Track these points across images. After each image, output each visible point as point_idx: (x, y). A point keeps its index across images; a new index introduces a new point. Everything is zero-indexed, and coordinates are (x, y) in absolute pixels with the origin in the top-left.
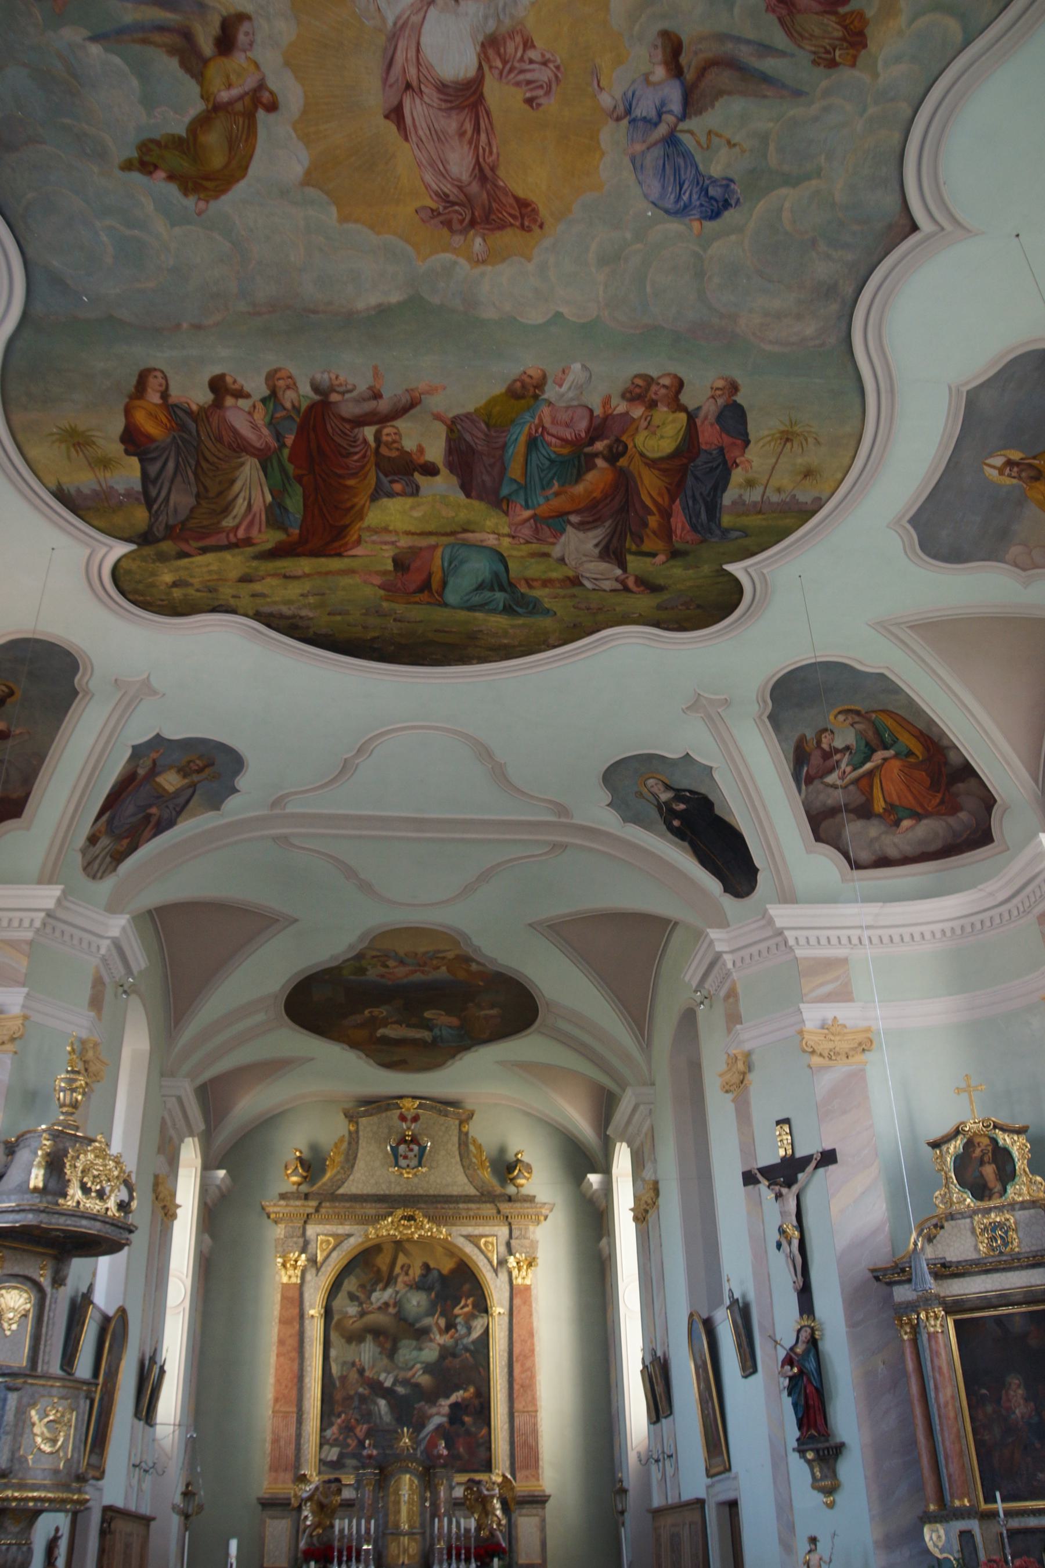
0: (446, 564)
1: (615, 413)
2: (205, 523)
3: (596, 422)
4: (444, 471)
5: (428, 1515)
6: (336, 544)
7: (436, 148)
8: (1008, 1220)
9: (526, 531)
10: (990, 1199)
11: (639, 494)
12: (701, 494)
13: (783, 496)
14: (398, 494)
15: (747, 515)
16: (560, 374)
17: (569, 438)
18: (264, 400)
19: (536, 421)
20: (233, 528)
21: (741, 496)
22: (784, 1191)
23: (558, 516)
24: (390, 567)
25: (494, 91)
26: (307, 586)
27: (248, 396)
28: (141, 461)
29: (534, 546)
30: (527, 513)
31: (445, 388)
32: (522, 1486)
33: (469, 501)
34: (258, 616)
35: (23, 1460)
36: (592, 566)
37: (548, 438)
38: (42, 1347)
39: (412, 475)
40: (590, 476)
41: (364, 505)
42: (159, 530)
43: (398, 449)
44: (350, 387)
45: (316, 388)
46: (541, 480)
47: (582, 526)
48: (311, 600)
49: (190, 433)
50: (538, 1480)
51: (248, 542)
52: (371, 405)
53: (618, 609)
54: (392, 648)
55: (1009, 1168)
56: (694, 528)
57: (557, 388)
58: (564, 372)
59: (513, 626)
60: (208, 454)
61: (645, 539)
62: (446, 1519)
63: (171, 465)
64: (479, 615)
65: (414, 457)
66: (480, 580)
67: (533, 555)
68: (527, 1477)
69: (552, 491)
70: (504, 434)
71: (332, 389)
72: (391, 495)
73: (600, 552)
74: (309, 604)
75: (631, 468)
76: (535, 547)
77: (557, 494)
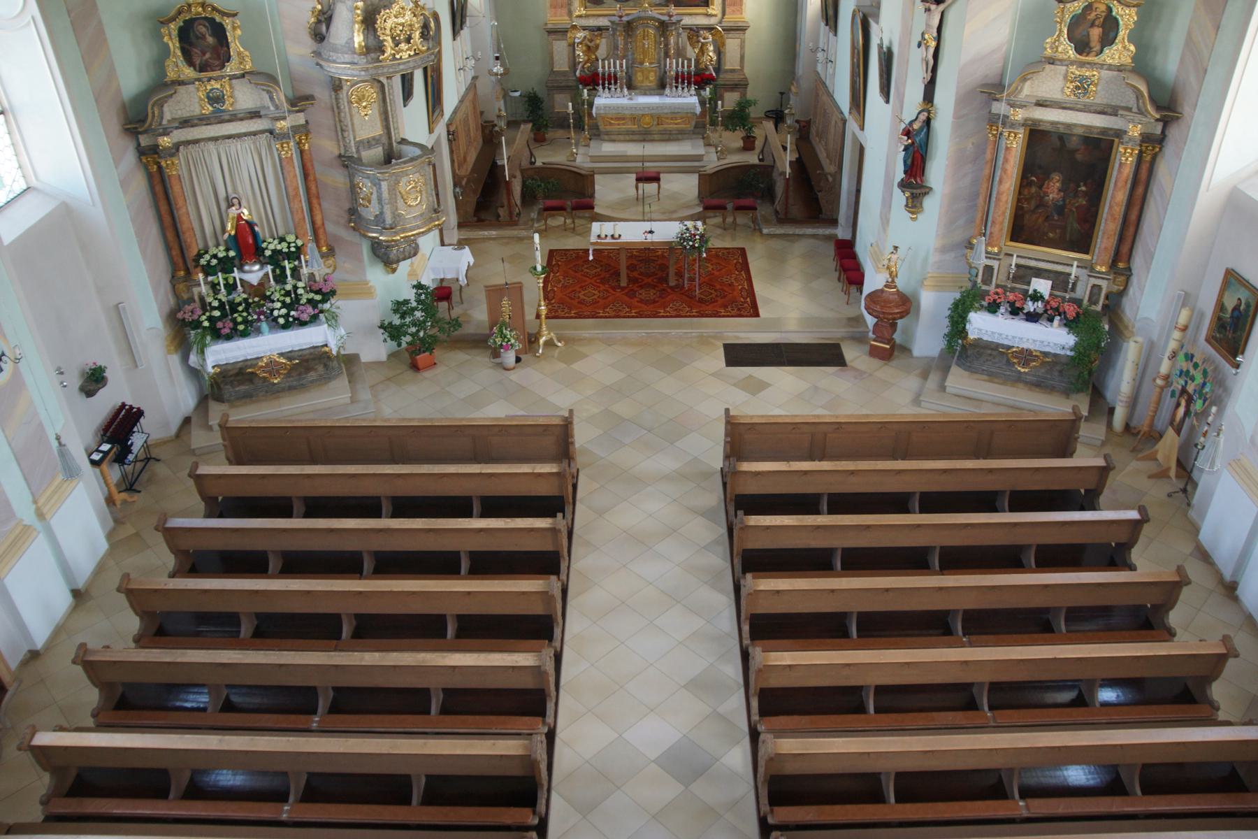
5: (662, 54)
8: (1094, 76)
10: (1088, 55)
22: (933, 7)
32: (731, 19)
35: (400, 215)
38: (391, 119)
50: (741, 14)
55: (1112, 35)
62: (674, 61)
68: (734, 11)
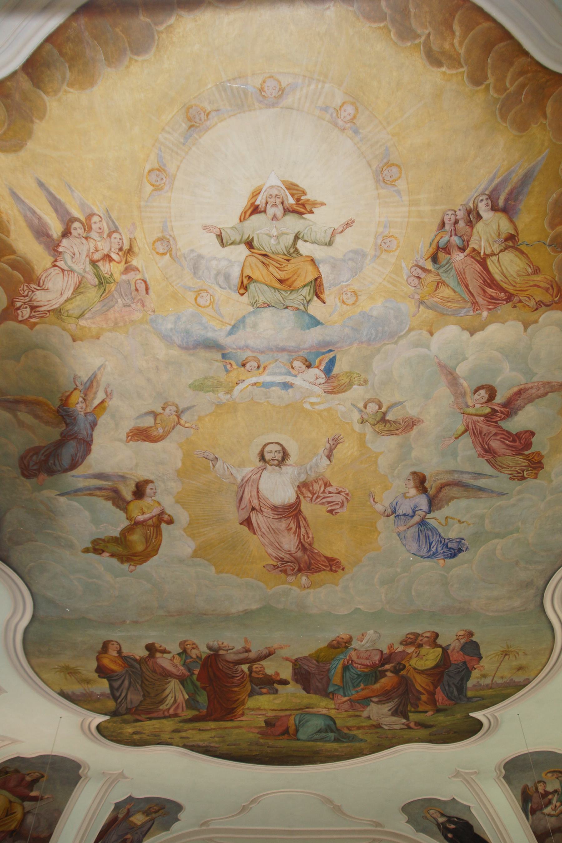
0: (297, 722)
1: (396, 651)
2: (149, 707)
3: (385, 656)
4: (292, 683)
6: (230, 716)
7: (274, 537)
9: (345, 706)
11: (414, 686)
12: (453, 683)
13: (505, 680)
14: (265, 694)
15: (483, 690)
16: (361, 636)
17: (369, 664)
18: (179, 654)
19: (348, 658)
20: (166, 710)
21: (478, 682)
23: (364, 699)
24: (263, 724)
25: (306, 508)
26: (213, 733)
27: (169, 652)
28: (109, 680)
29: (350, 712)
30: (345, 699)
31: (289, 646)
33: (309, 695)
34: (185, 746)
36: (387, 719)
37: (355, 665)
39: (273, 685)
40: (383, 680)
41: (245, 699)
42: (123, 709)
43: (263, 674)
44: (230, 648)
45: (210, 648)
46: (353, 684)
47: (379, 702)
48: (217, 739)
49: (136, 669)
51: (176, 715)
52: (246, 655)
53: (405, 737)
54: (268, 759)
56: (450, 699)
57: (359, 642)
58: (363, 635)
59: (340, 747)
60: (148, 678)
61: (419, 705)
63: (126, 683)
64: (318, 743)
65: (274, 677)
66: (319, 728)
67: (350, 716)
69: (360, 688)
70: (328, 665)
71: (220, 649)
72: (261, 694)
73: (392, 713)
74: (216, 741)
75: (409, 675)
76: (351, 713)
77: (363, 689)
